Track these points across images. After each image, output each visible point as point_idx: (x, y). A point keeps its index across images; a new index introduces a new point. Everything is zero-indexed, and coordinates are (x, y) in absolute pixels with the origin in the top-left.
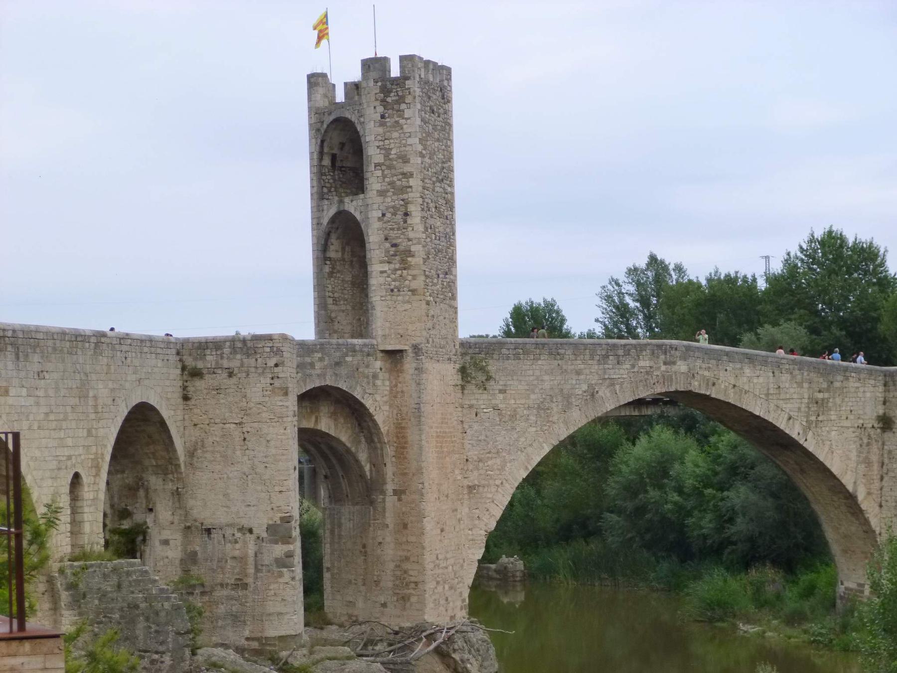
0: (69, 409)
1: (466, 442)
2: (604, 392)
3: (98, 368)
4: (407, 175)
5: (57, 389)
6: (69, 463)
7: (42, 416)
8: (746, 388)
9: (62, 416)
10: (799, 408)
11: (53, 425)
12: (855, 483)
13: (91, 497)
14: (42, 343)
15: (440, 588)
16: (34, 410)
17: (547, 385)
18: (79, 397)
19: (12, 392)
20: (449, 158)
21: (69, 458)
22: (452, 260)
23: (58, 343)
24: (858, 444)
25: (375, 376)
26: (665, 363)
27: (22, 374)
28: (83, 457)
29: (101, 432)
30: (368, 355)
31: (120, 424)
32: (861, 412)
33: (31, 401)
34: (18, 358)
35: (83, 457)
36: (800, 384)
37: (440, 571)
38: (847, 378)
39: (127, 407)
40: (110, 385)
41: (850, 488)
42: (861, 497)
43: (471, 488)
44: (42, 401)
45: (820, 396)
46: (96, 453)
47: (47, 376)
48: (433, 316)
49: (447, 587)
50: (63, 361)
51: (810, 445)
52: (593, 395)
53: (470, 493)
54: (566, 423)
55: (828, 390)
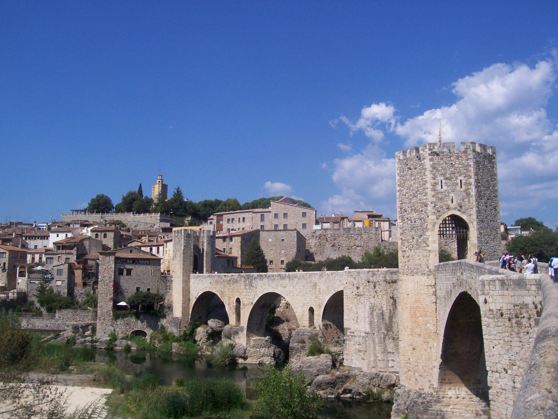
0: (308, 291)
3: (321, 281)
5: (304, 287)
6: (308, 304)
7: (297, 293)
9: (305, 293)
11: (302, 295)
13: (317, 313)
14: (298, 276)
16: (295, 291)
18: (313, 289)
19: (287, 287)
23: (304, 276)
27: (291, 283)
29: (321, 298)
33: (294, 289)
34: (290, 280)
37: (411, 366)
40: (326, 285)
47: (299, 283)
48: (408, 256)
49: (417, 374)
50: (306, 280)
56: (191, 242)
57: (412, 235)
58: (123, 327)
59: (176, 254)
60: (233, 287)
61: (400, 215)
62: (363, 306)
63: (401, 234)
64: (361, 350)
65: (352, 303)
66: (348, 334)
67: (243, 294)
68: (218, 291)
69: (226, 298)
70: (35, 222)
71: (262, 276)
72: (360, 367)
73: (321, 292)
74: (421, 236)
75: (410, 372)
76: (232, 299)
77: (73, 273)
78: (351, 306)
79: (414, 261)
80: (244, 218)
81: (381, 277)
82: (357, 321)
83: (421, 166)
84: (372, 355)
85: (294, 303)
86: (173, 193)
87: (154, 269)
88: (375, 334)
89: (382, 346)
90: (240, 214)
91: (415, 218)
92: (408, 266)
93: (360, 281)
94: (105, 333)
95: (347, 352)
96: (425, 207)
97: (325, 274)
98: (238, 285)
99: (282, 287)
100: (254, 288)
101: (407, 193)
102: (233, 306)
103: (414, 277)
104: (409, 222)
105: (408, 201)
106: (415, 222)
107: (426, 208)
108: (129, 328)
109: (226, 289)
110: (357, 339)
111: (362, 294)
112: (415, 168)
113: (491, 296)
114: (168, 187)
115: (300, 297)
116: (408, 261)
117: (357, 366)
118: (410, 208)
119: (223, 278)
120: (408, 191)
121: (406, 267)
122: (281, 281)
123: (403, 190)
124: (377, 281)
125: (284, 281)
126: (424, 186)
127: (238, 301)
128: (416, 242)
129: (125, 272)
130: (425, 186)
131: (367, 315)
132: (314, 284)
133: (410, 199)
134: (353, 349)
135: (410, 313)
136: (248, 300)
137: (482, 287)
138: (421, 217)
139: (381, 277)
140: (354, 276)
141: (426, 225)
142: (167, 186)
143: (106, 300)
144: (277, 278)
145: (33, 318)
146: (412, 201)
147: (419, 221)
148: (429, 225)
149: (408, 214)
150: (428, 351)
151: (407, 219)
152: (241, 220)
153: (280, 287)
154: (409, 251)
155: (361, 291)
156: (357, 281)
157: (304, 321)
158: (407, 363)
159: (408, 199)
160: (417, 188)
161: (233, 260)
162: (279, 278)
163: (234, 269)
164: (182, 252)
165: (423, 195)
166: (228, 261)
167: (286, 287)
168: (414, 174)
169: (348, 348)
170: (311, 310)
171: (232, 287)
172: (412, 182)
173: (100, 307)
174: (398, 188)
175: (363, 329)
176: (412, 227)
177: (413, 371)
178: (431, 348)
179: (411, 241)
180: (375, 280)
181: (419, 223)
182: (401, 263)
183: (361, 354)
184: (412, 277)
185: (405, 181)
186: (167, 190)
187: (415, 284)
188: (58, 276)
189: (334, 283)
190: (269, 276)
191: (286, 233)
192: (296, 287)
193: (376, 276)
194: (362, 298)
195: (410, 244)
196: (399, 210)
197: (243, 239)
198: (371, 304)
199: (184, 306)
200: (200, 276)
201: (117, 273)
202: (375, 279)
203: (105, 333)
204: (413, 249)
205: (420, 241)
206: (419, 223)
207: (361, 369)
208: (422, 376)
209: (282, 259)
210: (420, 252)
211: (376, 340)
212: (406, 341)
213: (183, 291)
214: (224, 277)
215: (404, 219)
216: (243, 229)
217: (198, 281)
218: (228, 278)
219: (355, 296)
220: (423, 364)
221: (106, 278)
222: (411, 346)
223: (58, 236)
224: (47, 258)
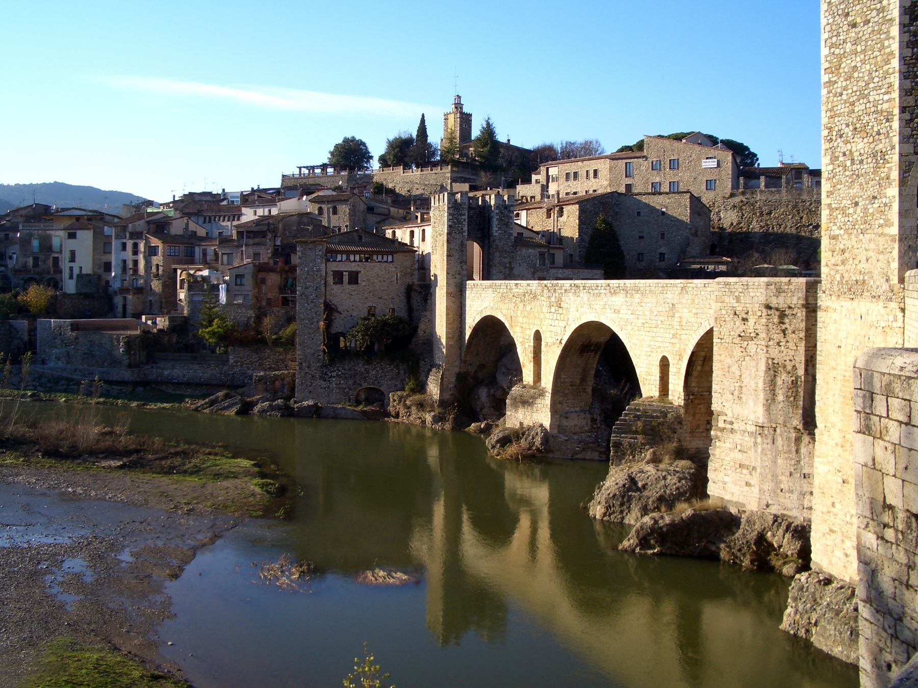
0: (659, 322)
3: (684, 301)
5: (652, 312)
6: (659, 350)
7: (640, 325)
9: (653, 326)
11: (648, 329)
14: (642, 289)
16: (635, 321)
19: (622, 312)
21: (659, 347)
23: (653, 288)
27: (629, 304)
28: (669, 348)
29: (683, 337)
31: (702, 334)
33: (633, 316)
35: (669, 348)
39: (710, 325)
40: (694, 311)
44: (640, 317)
46: (680, 348)
47: (643, 304)
48: (843, 251)
56: (463, 217)
58: (342, 382)
59: (436, 241)
60: (529, 309)
61: (828, 146)
62: (753, 363)
63: (830, 193)
64: (747, 463)
65: (731, 356)
66: (721, 424)
67: (546, 323)
69: (518, 329)
70: (224, 190)
71: (577, 286)
72: (741, 501)
73: (684, 324)
74: (875, 198)
75: (833, 535)
76: (528, 332)
77: (263, 281)
78: (729, 361)
79: (856, 262)
80: (595, 172)
81: (795, 298)
82: (740, 398)
83: (881, 15)
84: (769, 477)
85: (633, 346)
86: (480, 128)
87: (401, 271)
88: (778, 430)
89: (791, 459)
90: (587, 162)
91: (862, 152)
92: (842, 277)
93: (748, 305)
94: (310, 392)
95: (717, 465)
96: (888, 120)
97: (691, 285)
99: (612, 311)
100: (564, 312)
101: (845, 89)
104: (848, 163)
105: (847, 110)
106: (861, 162)
107: (887, 124)
108: (353, 385)
109: (519, 312)
110: (737, 438)
111: (752, 335)
112: (867, 22)
113: (890, 447)
114: (473, 118)
115: (644, 333)
116: (843, 263)
117: (735, 500)
118: (851, 127)
119: (514, 290)
120: (848, 82)
121: (838, 278)
122: (610, 299)
123: (836, 82)
124: (786, 306)
125: (614, 298)
126: (885, 68)
127: (538, 337)
128: (862, 215)
129: (346, 278)
130: (888, 66)
131: (761, 385)
132: (671, 306)
133: (853, 104)
134: (728, 458)
135: (841, 391)
136: (553, 336)
137: (864, 396)
138: (877, 148)
139: (795, 298)
140: (737, 294)
141: (886, 170)
142: (470, 115)
143: (311, 331)
144: (604, 291)
145: (192, 364)
146: (856, 109)
147: (870, 160)
148: (894, 168)
149: (847, 142)
151: (844, 154)
152: (591, 174)
153: (608, 311)
154: (846, 237)
155: (751, 328)
156: (743, 305)
157: (649, 387)
158: (829, 512)
159: (847, 105)
161: (552, 251)
162: (608, 291)
163: (554, 271)
164: (445, 238)
165: (883, 91)
166: (542, 255)
167: (619, 312)
168: (864, 38)
169: (717, 456)
170: (664, 364)
172: (858, 59)
173: (300, 344)
175: (752, 417)
176: (855, 176)
177: (840, 534)
180: (782, 306)
181: (871, 165)
182: (827, 265)
183: (745, 471)
184: (850, 302)
185: (840, 57)
186: (471, 124)
187: (855, 320)
188: (237, 287)
189: (708, 306)
190: (590, 288)
191: (669, 199)
192: (638, 312)
193: (784, 294)
194: (752, 347)
195: (847, 219)
196: (825, 132)
197: (582, 212)
198: (773, 359)
199: (450, 343)
201: (330, 280)
202: (779, 302)
203: (310, 392)
204: (855, 231)
205: (871, 211)
206: (871, 165)
207: (744, 505)
209: (663, 250)
210: (870, 241)
211: (779, 442)
212: (830, 458)
213: (447, 314)
214: (514, 287)
215: (836, 154)
216: (595, 191)
217: (473, 295)
218: (521, 291)
219: (738, 340)
221: (311, 289)
222: (840, 474)
223: (255, 212)
224: (223, 254)
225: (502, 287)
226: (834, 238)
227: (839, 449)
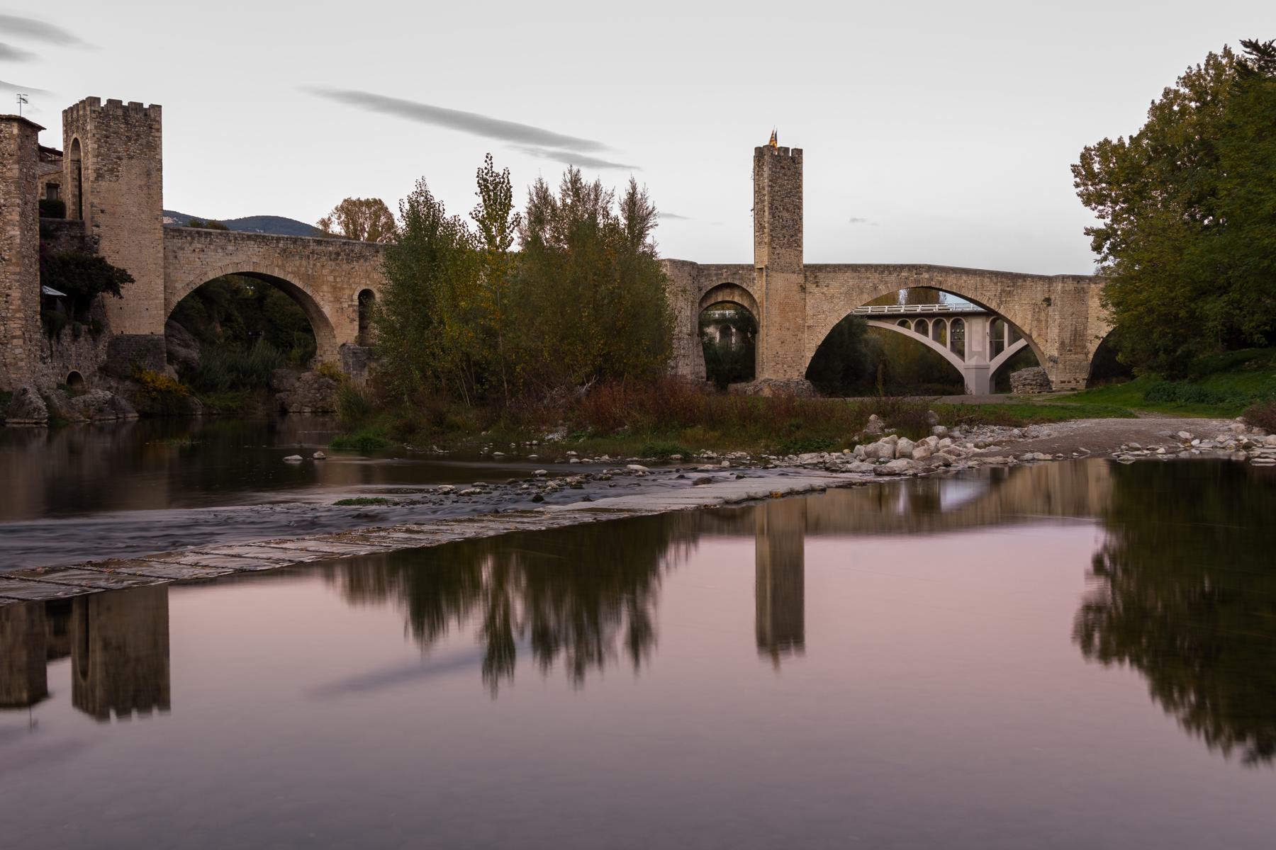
1: (807, 307)
2: (881, 287)
4: (764, 195)
8: (963, 285)
10: (995, 295)
12: (1030, 330)
15: (779, 366)
17: (851, 284)
20: (800, 186)
22: (800, 231)
24: (1032, 312)
25: (754, 279)
26: (916, 274)
30: (750, 270)
32: (1034, 297)
36: (996, 284)
38: (1025, 281)
41: (1028, 332)
42: (1034, 337)
43: (809, 327)
45: (1009, 289)
51: (1002, 311)
52: (875, 288)
53: (808, 329)
54: (861, 300)
55: (1013, 286)
57: (784, 234)
68: (292, 273)
76: (347, 292)
98: (367, 264)
102: (349, 306)
103: (784, 275)
104: (781, 220)
112: (789, 169)
116: (779, 258)
150: (798, 342)
160: (791, 189)
171: (345, 266)
174: (770, 183)
178: (799, 340)
179: (782, 239)
185: (777, 178)
200: (210, 234)
208: (790, 367)
212: (774, 335)
218: (331, 249)
220: (792, 356)
225: (282, 242)
226: (775, 248)
227: (780, 331)
